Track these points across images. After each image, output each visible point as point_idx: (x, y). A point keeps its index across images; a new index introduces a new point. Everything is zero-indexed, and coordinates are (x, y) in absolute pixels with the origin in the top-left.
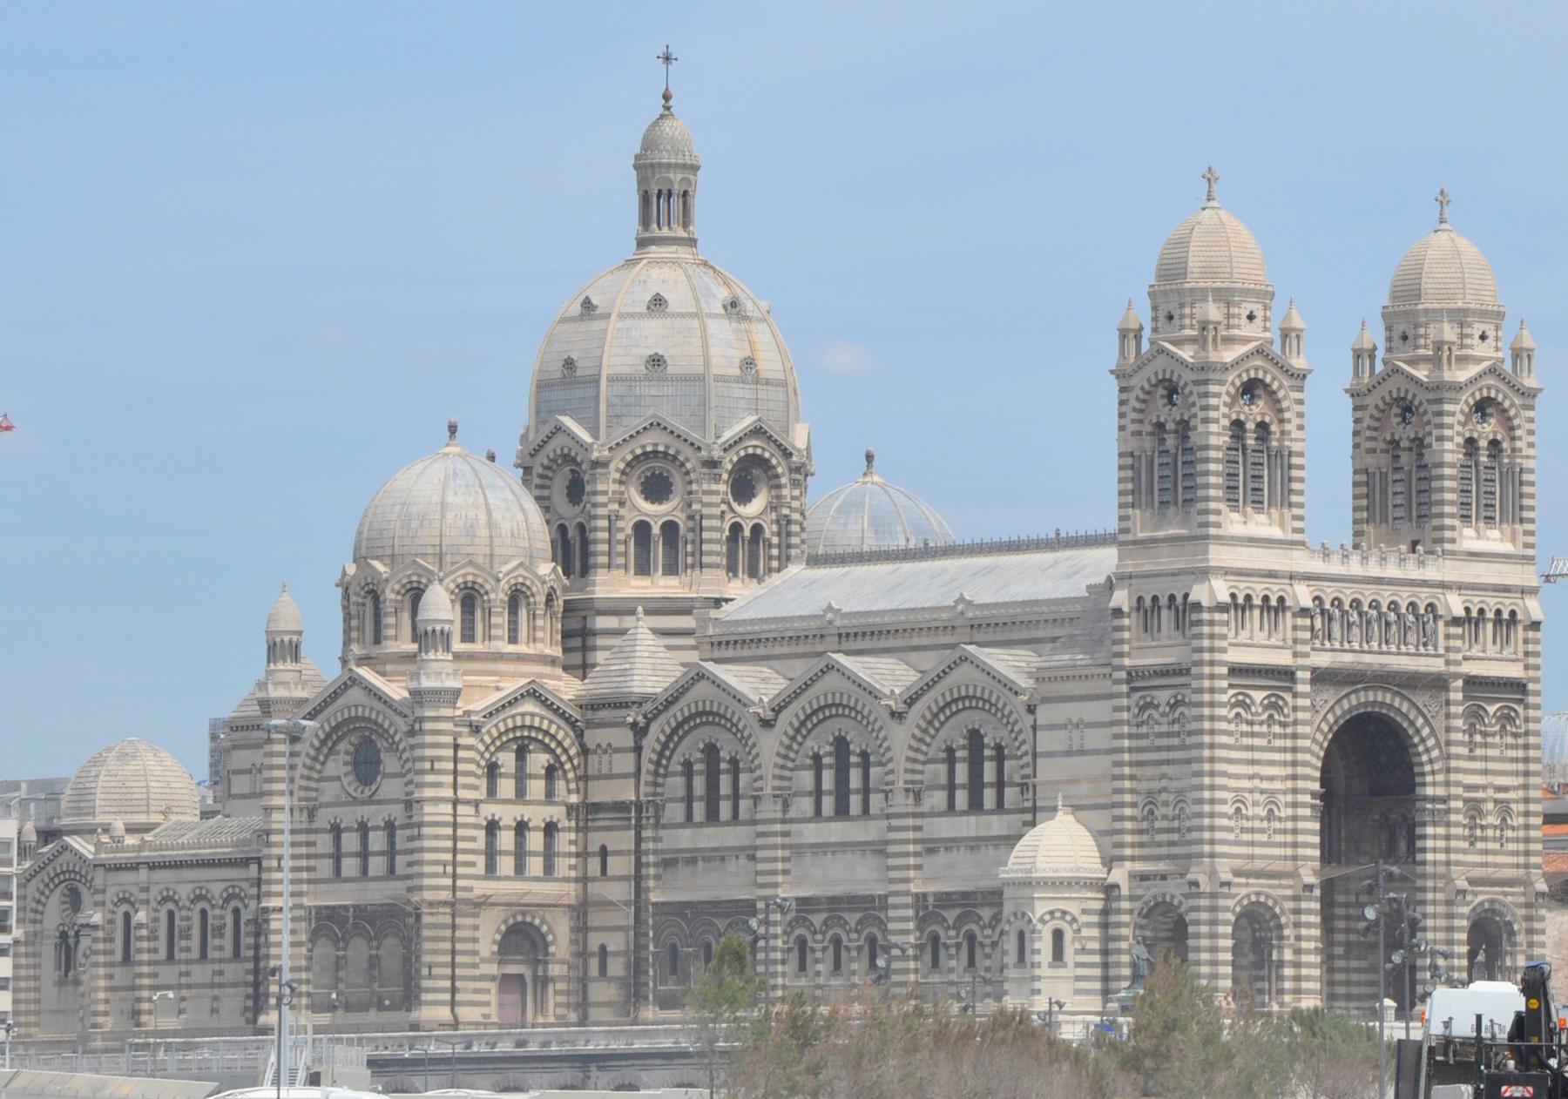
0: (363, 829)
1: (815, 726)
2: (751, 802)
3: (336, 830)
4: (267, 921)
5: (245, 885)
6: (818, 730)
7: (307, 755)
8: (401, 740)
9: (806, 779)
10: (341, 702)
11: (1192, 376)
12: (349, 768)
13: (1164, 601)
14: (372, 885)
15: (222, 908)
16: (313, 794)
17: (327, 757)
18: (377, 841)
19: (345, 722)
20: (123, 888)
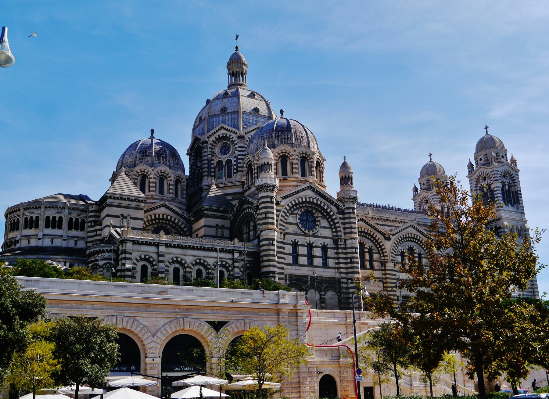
0: (310, 247)
1: (403, 242)
2: (379, 264)
3: (295, 245)
4: (274, 277)
5: (230, 262)
6: (403, 244)
7: (283, 212)
8: (334, 214)
9: (399, 259)
10: (301, 194)
11: (515, 173)
12: (299, 221)
13: (515, 227)
14: (316, 269)
15: (213, 269)
16: (284, 228)
17: (290, 214)
18: (317, 252)
19: (303, 202)
20: (144, 253)
